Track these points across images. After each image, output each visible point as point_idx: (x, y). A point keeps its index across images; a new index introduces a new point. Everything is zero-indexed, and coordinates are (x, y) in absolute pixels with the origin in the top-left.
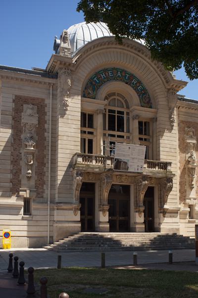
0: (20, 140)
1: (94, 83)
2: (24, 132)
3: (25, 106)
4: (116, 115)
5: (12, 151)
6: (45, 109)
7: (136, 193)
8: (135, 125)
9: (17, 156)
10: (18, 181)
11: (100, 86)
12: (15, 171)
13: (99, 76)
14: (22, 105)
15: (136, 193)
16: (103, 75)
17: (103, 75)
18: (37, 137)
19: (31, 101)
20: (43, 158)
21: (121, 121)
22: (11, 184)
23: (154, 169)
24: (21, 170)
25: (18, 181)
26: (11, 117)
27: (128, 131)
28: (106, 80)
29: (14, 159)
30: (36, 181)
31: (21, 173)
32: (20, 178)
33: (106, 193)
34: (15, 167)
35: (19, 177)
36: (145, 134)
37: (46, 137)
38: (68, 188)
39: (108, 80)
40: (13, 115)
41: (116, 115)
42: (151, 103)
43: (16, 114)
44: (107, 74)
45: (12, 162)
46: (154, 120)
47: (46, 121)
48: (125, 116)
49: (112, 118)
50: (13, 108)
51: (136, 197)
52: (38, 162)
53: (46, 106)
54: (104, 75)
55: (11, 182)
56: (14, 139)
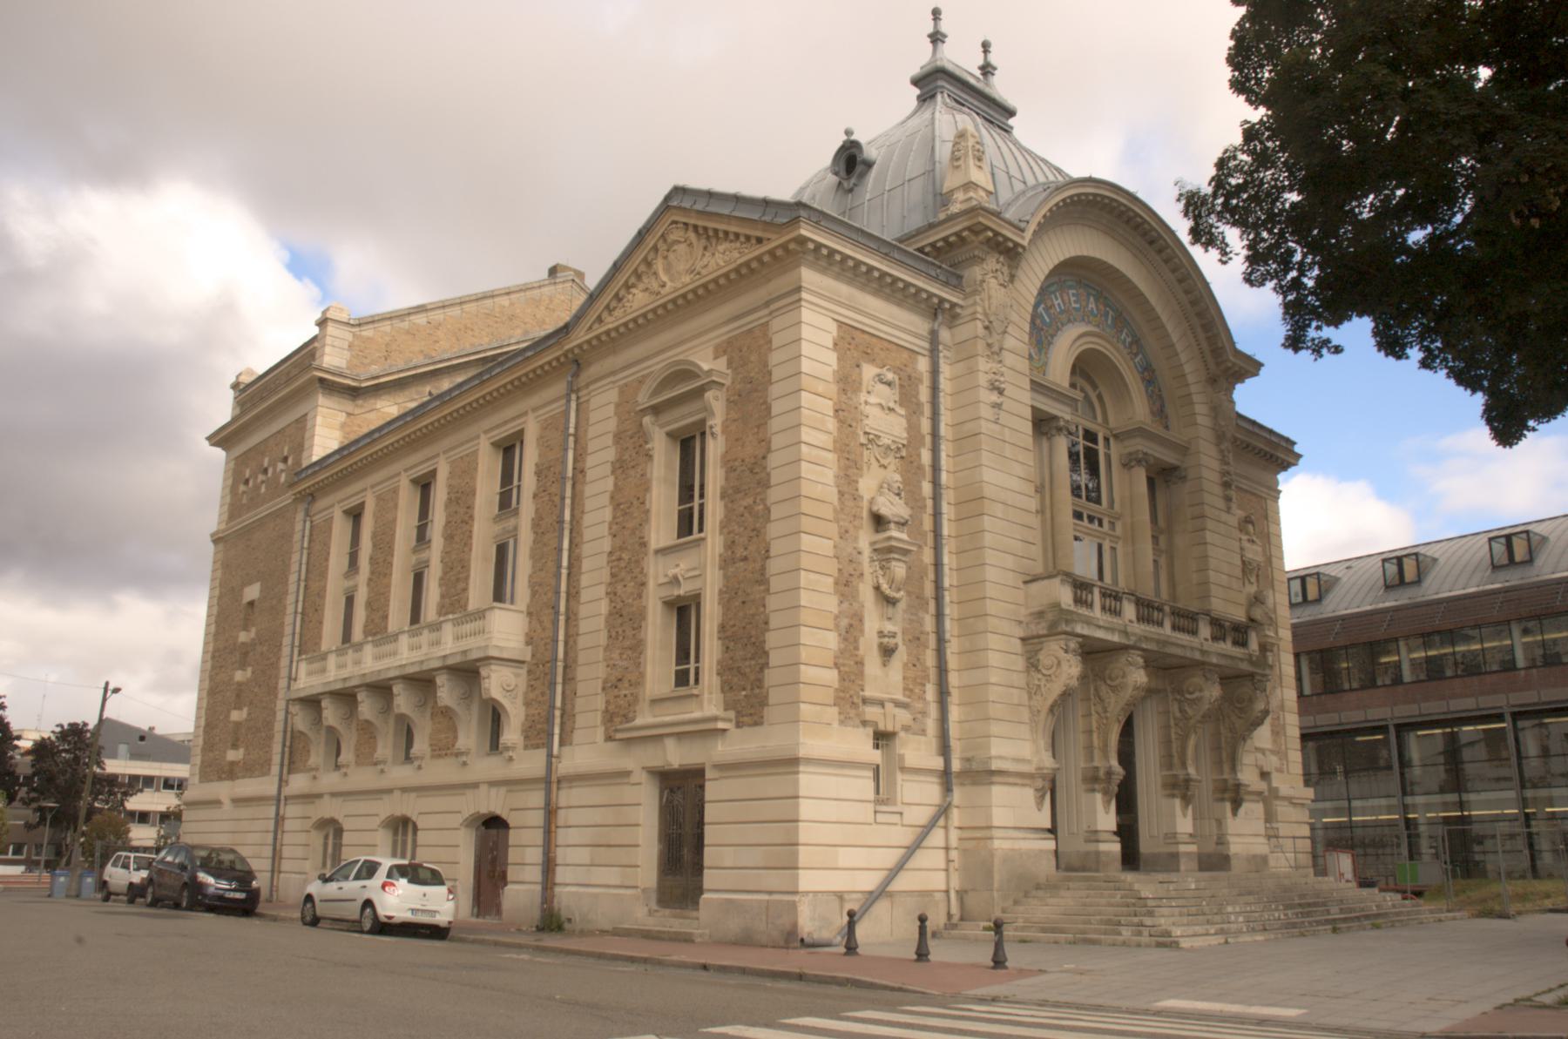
0: (856, 498)
2: (865, 468)
5: (837, 538)
7: (1167, 727)
10: (857, 663)
11: (1053, 336)
12: (844, 622)
13: (1049, 304)
14: (858, 366)
16: (1057, 299)
20: (922, 578)
22: (835, 673)
24: (861, 620)
25: (857, 663)
26: (831, 403)
28: (1064, 317)
29: (840, 570)
30: (905, 665)
31: (862, 631)
32: (861, 652)
34: (845, 605)
35: (857, 648)
38: (1016, 702)
39: (1069, 321)
42: (1167, 417)
43: (844, 398)
44: (1066, 298)
45: (836, 583)
50: (834, 371)
54: (1060, 301)
55: (836, 665)
56: (841, 494)
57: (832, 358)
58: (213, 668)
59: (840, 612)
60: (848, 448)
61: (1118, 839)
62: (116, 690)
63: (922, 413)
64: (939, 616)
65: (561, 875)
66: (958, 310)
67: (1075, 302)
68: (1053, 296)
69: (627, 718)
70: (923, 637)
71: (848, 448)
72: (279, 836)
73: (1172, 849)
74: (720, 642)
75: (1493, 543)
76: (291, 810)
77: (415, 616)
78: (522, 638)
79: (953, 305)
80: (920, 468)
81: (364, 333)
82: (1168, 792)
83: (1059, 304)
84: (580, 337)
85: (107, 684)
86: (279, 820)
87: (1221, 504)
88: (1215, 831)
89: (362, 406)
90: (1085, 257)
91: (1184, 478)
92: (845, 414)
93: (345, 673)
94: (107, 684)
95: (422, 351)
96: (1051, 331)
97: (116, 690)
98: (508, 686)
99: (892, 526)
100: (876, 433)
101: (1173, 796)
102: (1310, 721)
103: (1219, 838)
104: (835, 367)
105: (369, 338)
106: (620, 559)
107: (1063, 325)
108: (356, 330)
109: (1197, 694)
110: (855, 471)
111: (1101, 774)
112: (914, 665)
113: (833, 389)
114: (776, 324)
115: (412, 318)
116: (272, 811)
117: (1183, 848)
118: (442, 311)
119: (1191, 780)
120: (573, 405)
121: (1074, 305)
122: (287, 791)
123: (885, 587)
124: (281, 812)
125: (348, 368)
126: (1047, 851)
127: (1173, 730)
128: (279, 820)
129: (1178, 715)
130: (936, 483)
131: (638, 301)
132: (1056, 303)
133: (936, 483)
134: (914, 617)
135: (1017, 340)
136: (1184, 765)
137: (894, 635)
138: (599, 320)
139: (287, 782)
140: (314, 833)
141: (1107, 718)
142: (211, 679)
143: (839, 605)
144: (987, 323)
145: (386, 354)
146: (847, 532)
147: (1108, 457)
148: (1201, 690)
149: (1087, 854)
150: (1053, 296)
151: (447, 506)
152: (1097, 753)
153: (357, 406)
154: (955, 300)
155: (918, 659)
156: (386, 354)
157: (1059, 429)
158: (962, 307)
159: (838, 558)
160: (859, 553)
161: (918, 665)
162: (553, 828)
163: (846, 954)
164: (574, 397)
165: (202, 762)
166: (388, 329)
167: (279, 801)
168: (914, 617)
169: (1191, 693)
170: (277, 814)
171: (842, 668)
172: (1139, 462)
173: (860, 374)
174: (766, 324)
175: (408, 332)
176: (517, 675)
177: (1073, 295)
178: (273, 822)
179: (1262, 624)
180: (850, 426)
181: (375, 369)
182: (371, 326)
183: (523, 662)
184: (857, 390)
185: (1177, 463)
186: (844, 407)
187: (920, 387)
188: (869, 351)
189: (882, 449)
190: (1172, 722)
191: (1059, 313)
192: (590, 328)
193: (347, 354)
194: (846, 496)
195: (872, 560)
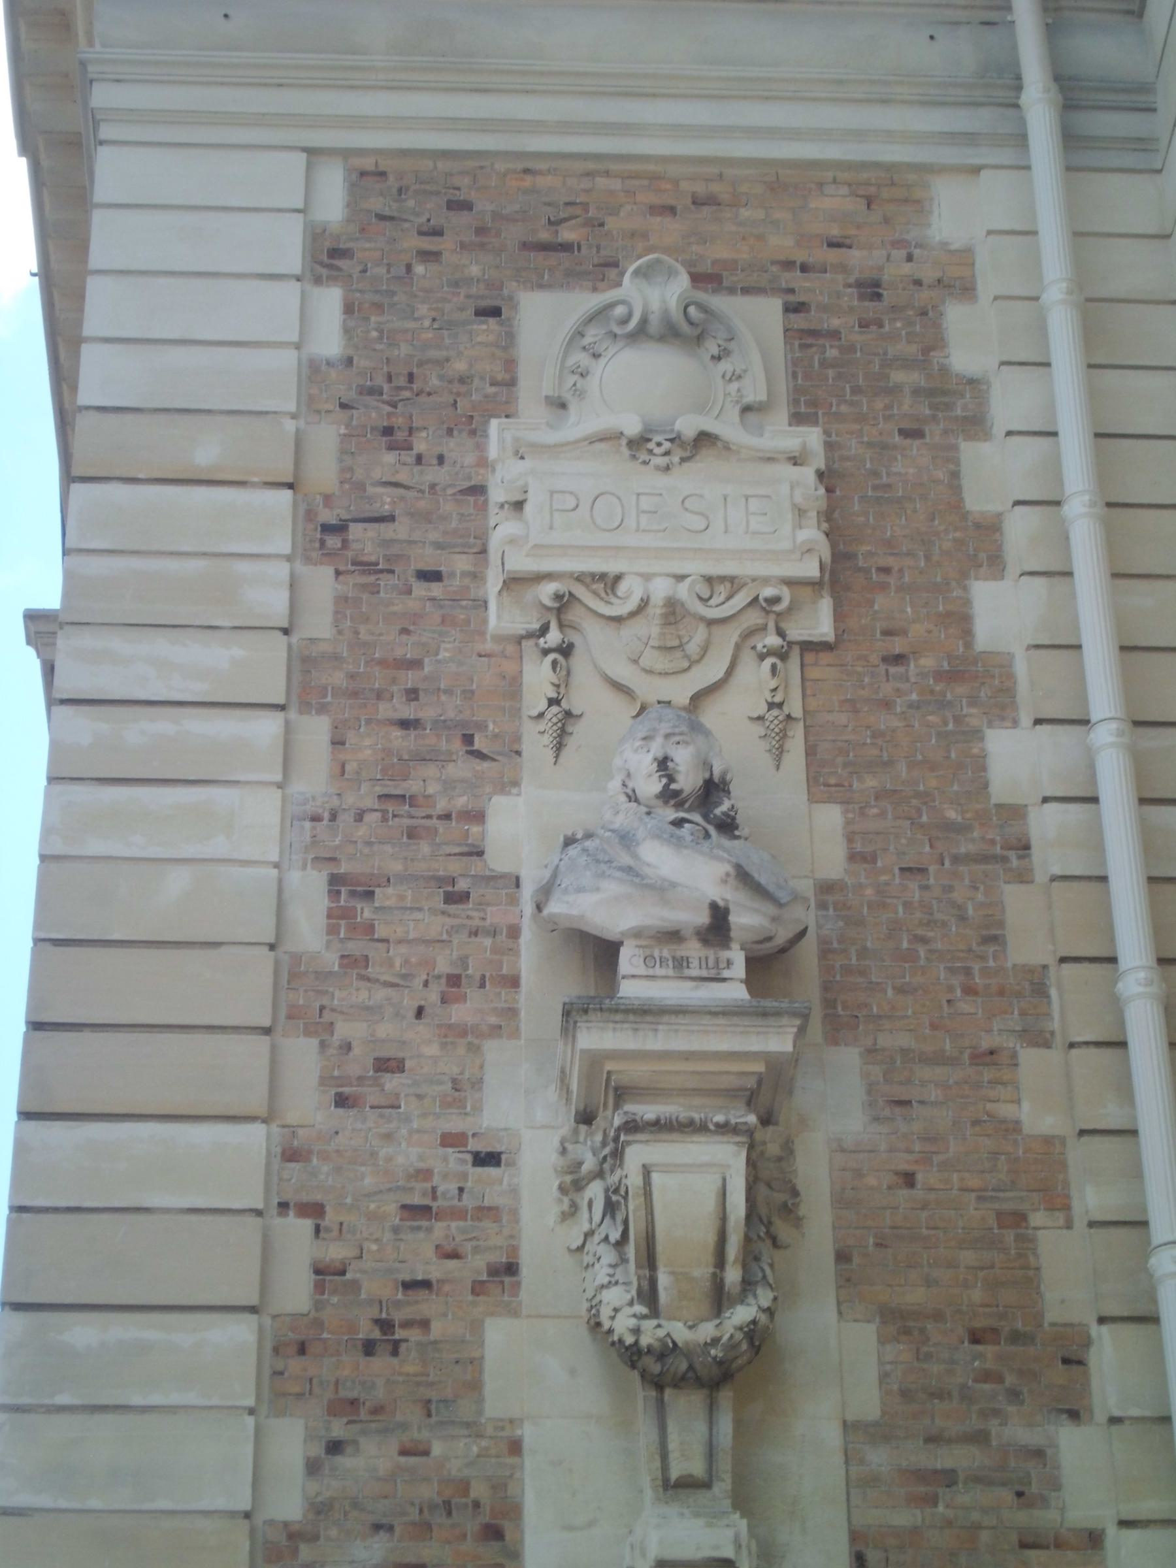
6: (935, 342)
9: (417, 1212)
18: (831, 817)
37: (1015, 812)
47: (991, 528)
53: (966, 290)
59: (320, 1509)
60: (410, 678)
71: (410, 678)
92: (400, 530)
99: (629, 960)
110: (462, 768)
143: (313, 1468)
146: (387, 1065)
159: (313, 1210)
173: (510, 338)
180: (431, 576)
186: (386, 500)
188: (567, 235)
189: (649, 628)
194: (385, 896)
195: (574, 1183)
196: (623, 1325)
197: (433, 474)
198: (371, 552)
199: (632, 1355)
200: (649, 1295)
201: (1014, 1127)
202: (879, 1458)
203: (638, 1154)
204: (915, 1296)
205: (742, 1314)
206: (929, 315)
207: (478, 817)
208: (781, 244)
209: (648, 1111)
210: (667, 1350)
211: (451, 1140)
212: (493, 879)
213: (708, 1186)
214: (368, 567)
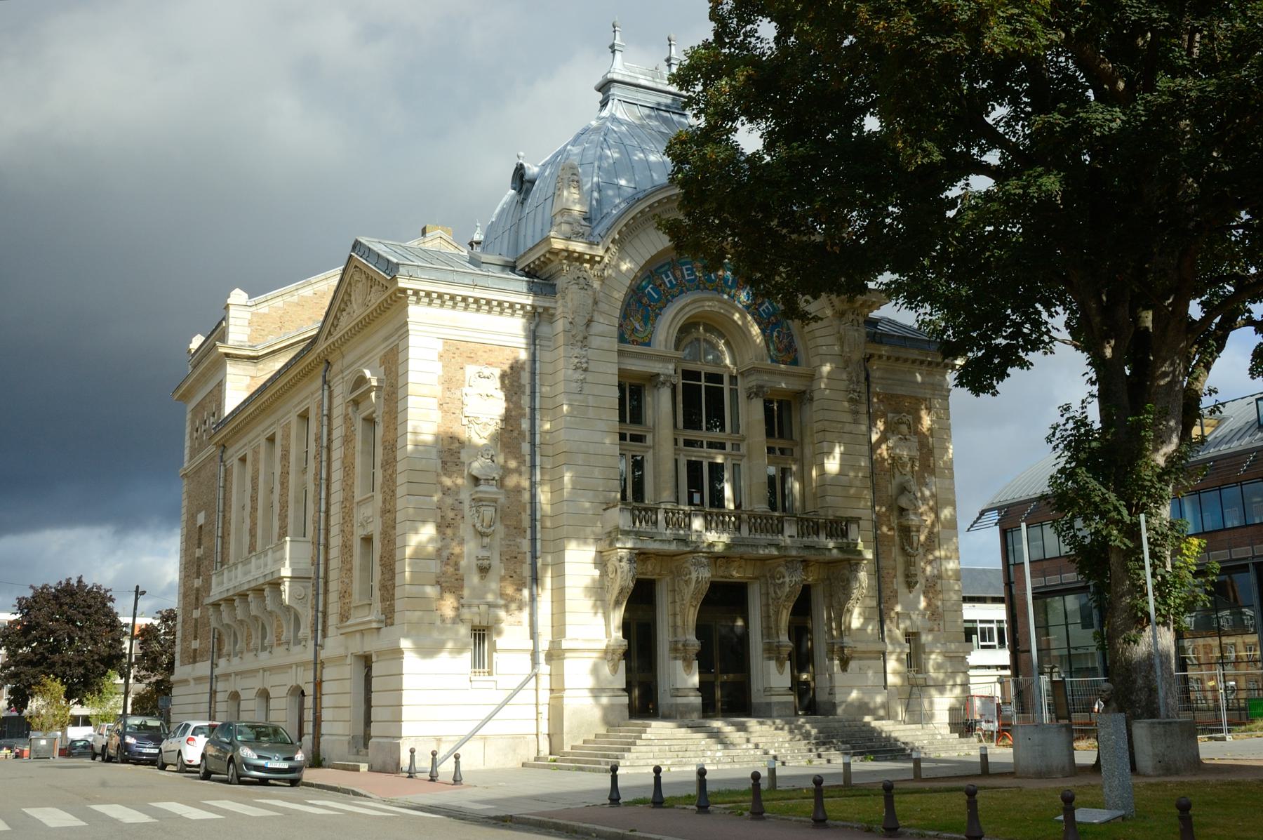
1: (645, 300)
3: (471, 370)
4: (703, 383)
7: (768, 605)
8: (752, 415)
11: (661, 309)
15: (768, 605)
16: (667, 276)
17: (667, 276)
19: (485, 356)
21: (716, 397)
23: (815, 539)
25: (457, 580)
27: (736, 428)
33: (692, 609)
36: (781, 436)
39: (682, 292)
40: (440, 394)
41: (703, 383)
42: (796, 350)
44: (678, 273)
46: (802, 397)
48: (726, 386)
49: (691, 395)
51: (766, 617)
52: (507, 526)
54: (671, 277)
55: (438, 583)
57: (438, 368)
58: (185, 577)
61: (700, 694)
62: (144, 593)
63: (524, 393)
64: (533, 540)
65: (325, 728)
66: (552, 311)
67: (688, 275)
68: (663, 276)
69: (348, 619)
70: (519, 556)
72: (213, 706)
73: (768, 700)
74: (380, 568)
75: (1259, 402)
76: (220, 686)
77: (252, 548)
78: (310, 561)
79: (546, 309)
80: (521, 433)
81: (260, 311)
82: (768, 655)
83: (670, 282)
84: (322, 346)
85: (138, 587)
86: (213, 693)
87: (848, 417)
88: (828, 684)
89: (262, 370)
90: (653, 258)
91: (811, 399)
92: (449, 405)
93: (226, 586)
94: (138, 587)
95: (310, 318)
96: (659, 305)
97: (144, 593)
98: (300, 595)
99: (482, 482)
100: (475, 415)
101: (770, 659)
102: (1041, 582)
103: (831, 690)
104: (441, 373)
105: (265, 314)
106: (345, 507)
107: (673, 297)
108: (253, 309)
109: (782, 580)
111: (680, 646)
112: (511, 577)
113: (438, 390)
114: (401, 344)
115: (300, 292)
116: (207, 687)
117: (775, 699)
118: (325, 282)
119: (781, 646)
120: (326, 393)
121: (687, 278)
122: (217, 671)
123: (478, 525)
124: (214, 688)
125: (249, 341)
126: (622, 705)
127: (771, 607)
128: (213, 693)
129: (774, 595)
130: (533, 444)
131: (346, 323)
132: (666, 280)
133: (533, 444)
134: (512, 543)
135: (607, 325)
136: (778, 636)
137: (488, 558)
138: (330, 333)
139: (216, 665)
140: (230, 702)
141: (684, 604)
142: (184, 585)
144: (570, 320)
145: (280, 325)
147: (734, 393)
148: (784, 577)
149: (672, 705)
150: (663, 276)
151: (281, 461)
152: (680, 630)
153: (258, 370)
154: (547, 305)
155: (515, 572)
156: (280, 325)
157: (663, 384)
158: (555, 308)
159: (440, 509)
160: (460, 503)
161: (514, 575)
162: (318, 696)
163: (408, 777)
164: (326, 387)
165: (182, 649)
166: (281, 304)
167: (212, 679)
168: (512, 543)
169: (779, 579)
170: (211, 689)
171: (443, 585)
172: (757, 395)
174: (397, 345)
175: (298, 304)
176: (305, 588)
177: (687, 270)
178: (208, 695)
179: (907, 510)
180: (454, 413)
181: (271, 339)
182: (266, 304)
183: (310, 578)
184: (460, 384)
185: (803, 388)
186: (448, 400)
187: (522, 373)
188: (472, 355)
190: (770, 601)
191: (673, 286)
192: (326, 339)
193: (248, 331)
194: (448, 464)
195: (471, 507)
196: (479, 529)
197: (455, 396)
198: (446, 409)
199: (480, 533)
200: (482, 525)
201: (520, 501)
202: (503, 542)
203: (483, 508)
204: (508, 523)
205: (493, 528)
206: (519, 373)
207: (459, 453)
208: (500, 359)
209: (484, 503)
210: (484, 533)
211: (457, 500)
212: (461, 463)
213: (490, 513)
214: (445, 411)
